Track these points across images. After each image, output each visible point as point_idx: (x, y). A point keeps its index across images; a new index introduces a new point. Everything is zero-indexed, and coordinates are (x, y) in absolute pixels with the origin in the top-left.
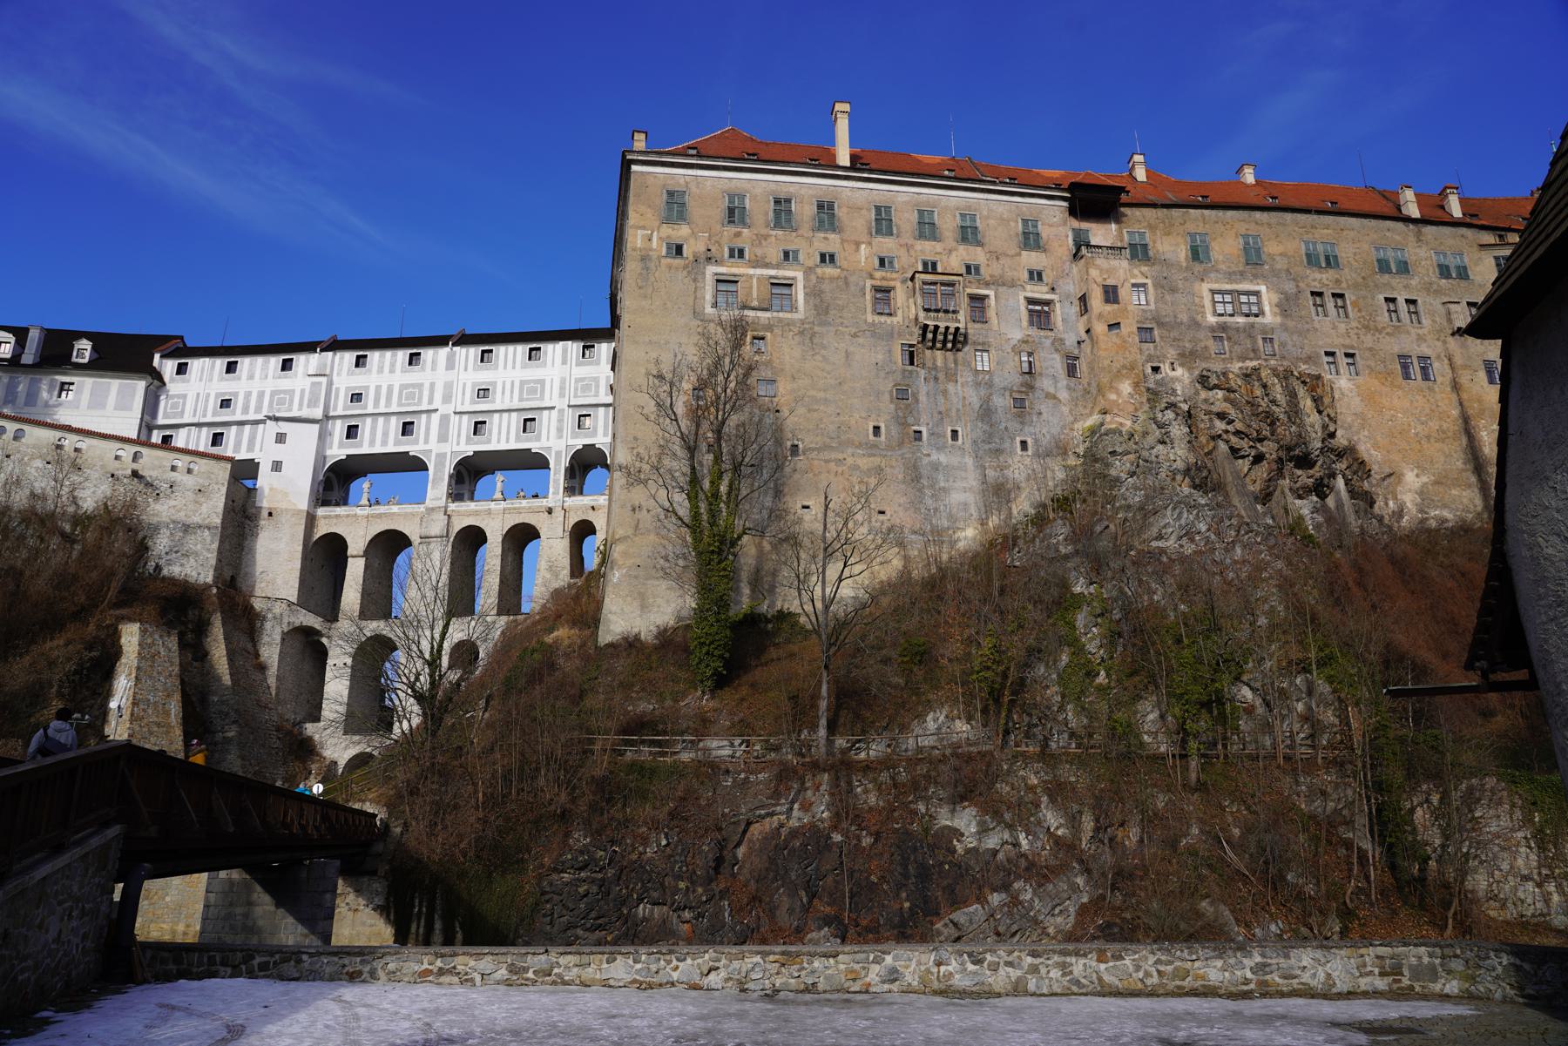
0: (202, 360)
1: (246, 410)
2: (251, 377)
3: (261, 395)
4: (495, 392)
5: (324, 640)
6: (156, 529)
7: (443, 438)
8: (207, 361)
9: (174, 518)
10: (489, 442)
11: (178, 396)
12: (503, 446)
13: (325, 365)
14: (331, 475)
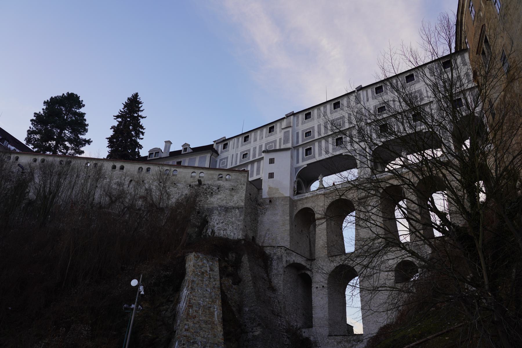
1: (254, 156)
5: (309, 273)
6: (211, 211)
9: (219, 204)
11: (224, 159)
13: (290, 123)
14: (299, 179)
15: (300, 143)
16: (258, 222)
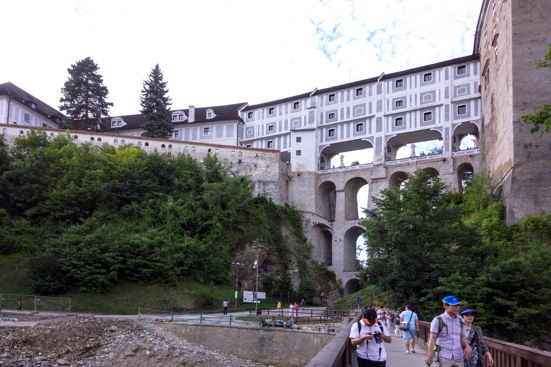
0: (258, 110)
1: (280, 129)
2: (281, 114)
3: (286, 121)
4: (406, 102)
7: (379, 129)
8: (260, 110)
10: (405, 128)
11: (250, 128)
12: (413, 129)
13: (315, 102)
15: (324, 124)
16: (288, 192)
